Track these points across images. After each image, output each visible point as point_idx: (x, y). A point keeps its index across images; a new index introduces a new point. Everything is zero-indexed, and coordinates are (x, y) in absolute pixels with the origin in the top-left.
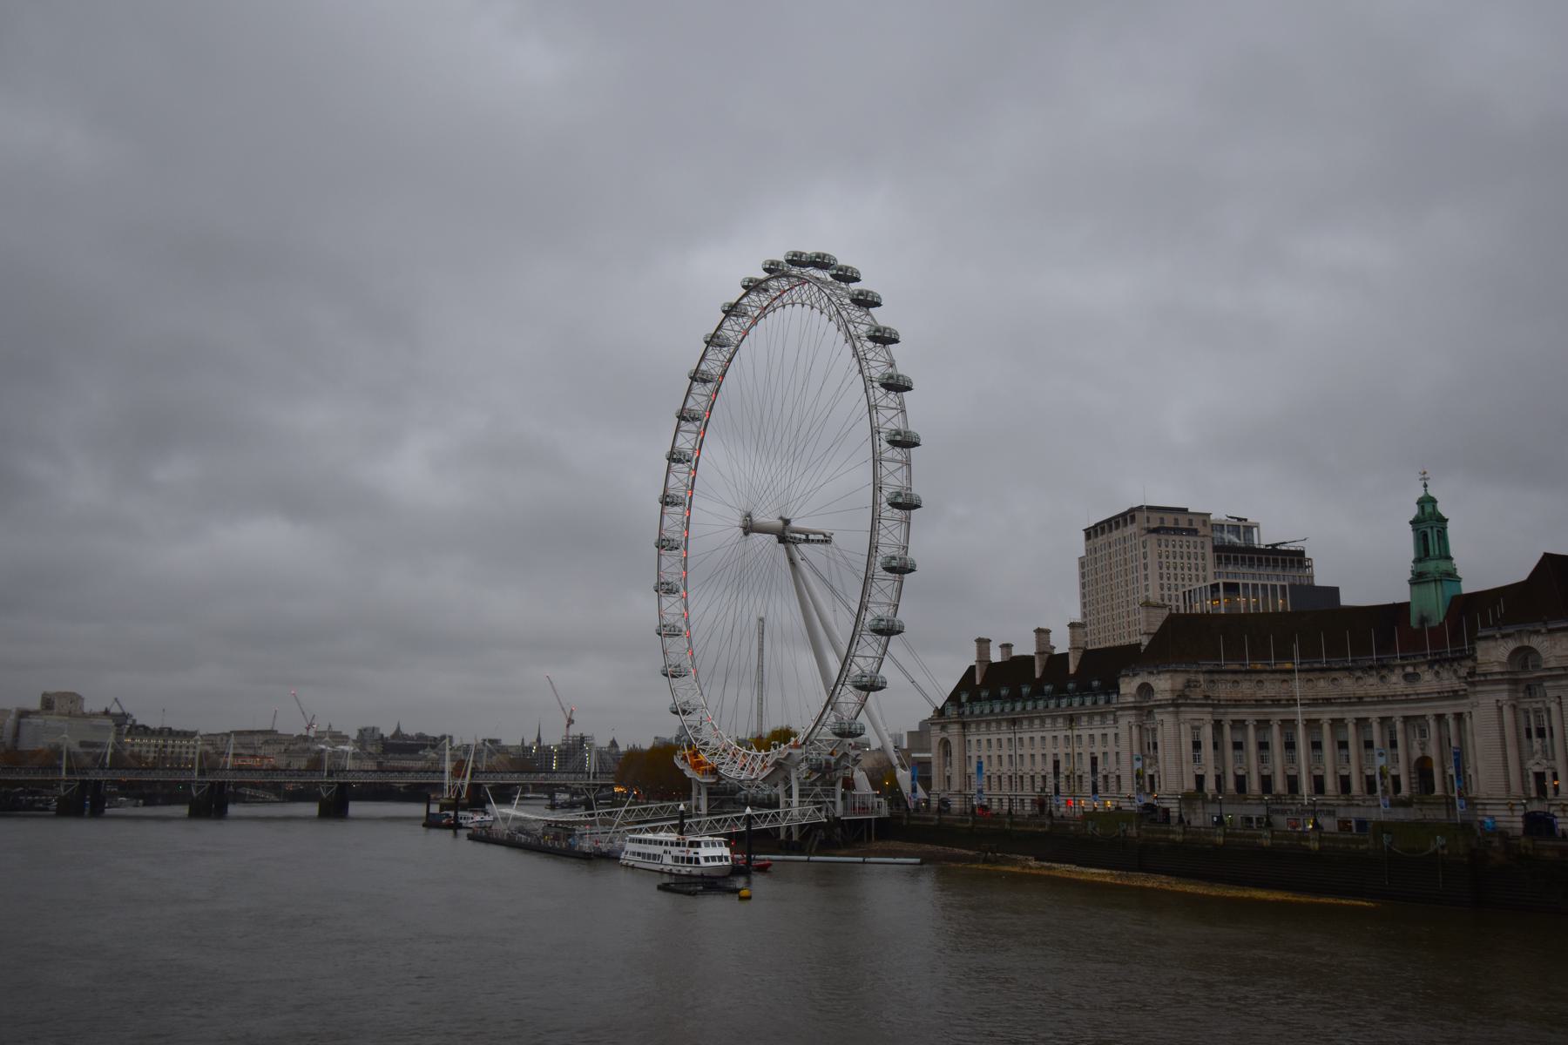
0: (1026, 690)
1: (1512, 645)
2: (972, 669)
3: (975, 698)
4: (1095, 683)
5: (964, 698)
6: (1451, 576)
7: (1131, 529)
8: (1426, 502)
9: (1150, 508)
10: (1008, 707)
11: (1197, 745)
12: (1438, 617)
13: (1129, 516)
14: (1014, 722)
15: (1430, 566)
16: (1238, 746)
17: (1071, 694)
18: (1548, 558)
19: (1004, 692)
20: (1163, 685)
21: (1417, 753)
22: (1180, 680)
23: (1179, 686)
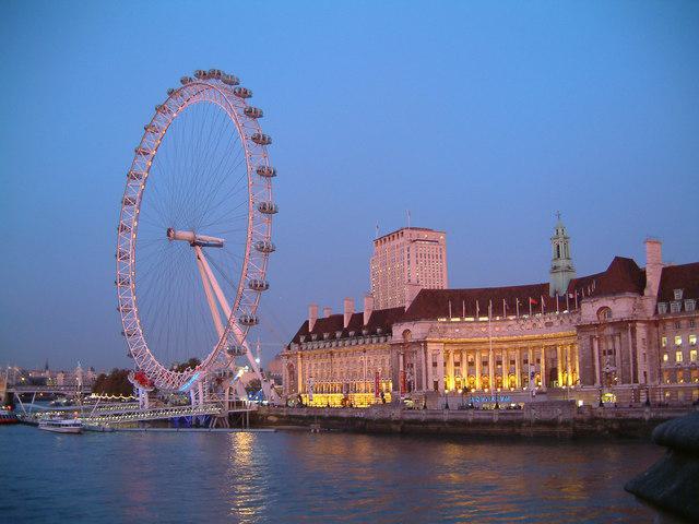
0: (338, 334)
1: (598, 305)
3: (308, 339)
7: (401, 240)
10: (328, 345)
11: (435, 365)
12: (563, 291)
13: (399, 233)
15: (562, 263)
16: (457, 364)
18: (617, 259)
20: (417, 330)
21: (550, 366)
23: (425, 330)
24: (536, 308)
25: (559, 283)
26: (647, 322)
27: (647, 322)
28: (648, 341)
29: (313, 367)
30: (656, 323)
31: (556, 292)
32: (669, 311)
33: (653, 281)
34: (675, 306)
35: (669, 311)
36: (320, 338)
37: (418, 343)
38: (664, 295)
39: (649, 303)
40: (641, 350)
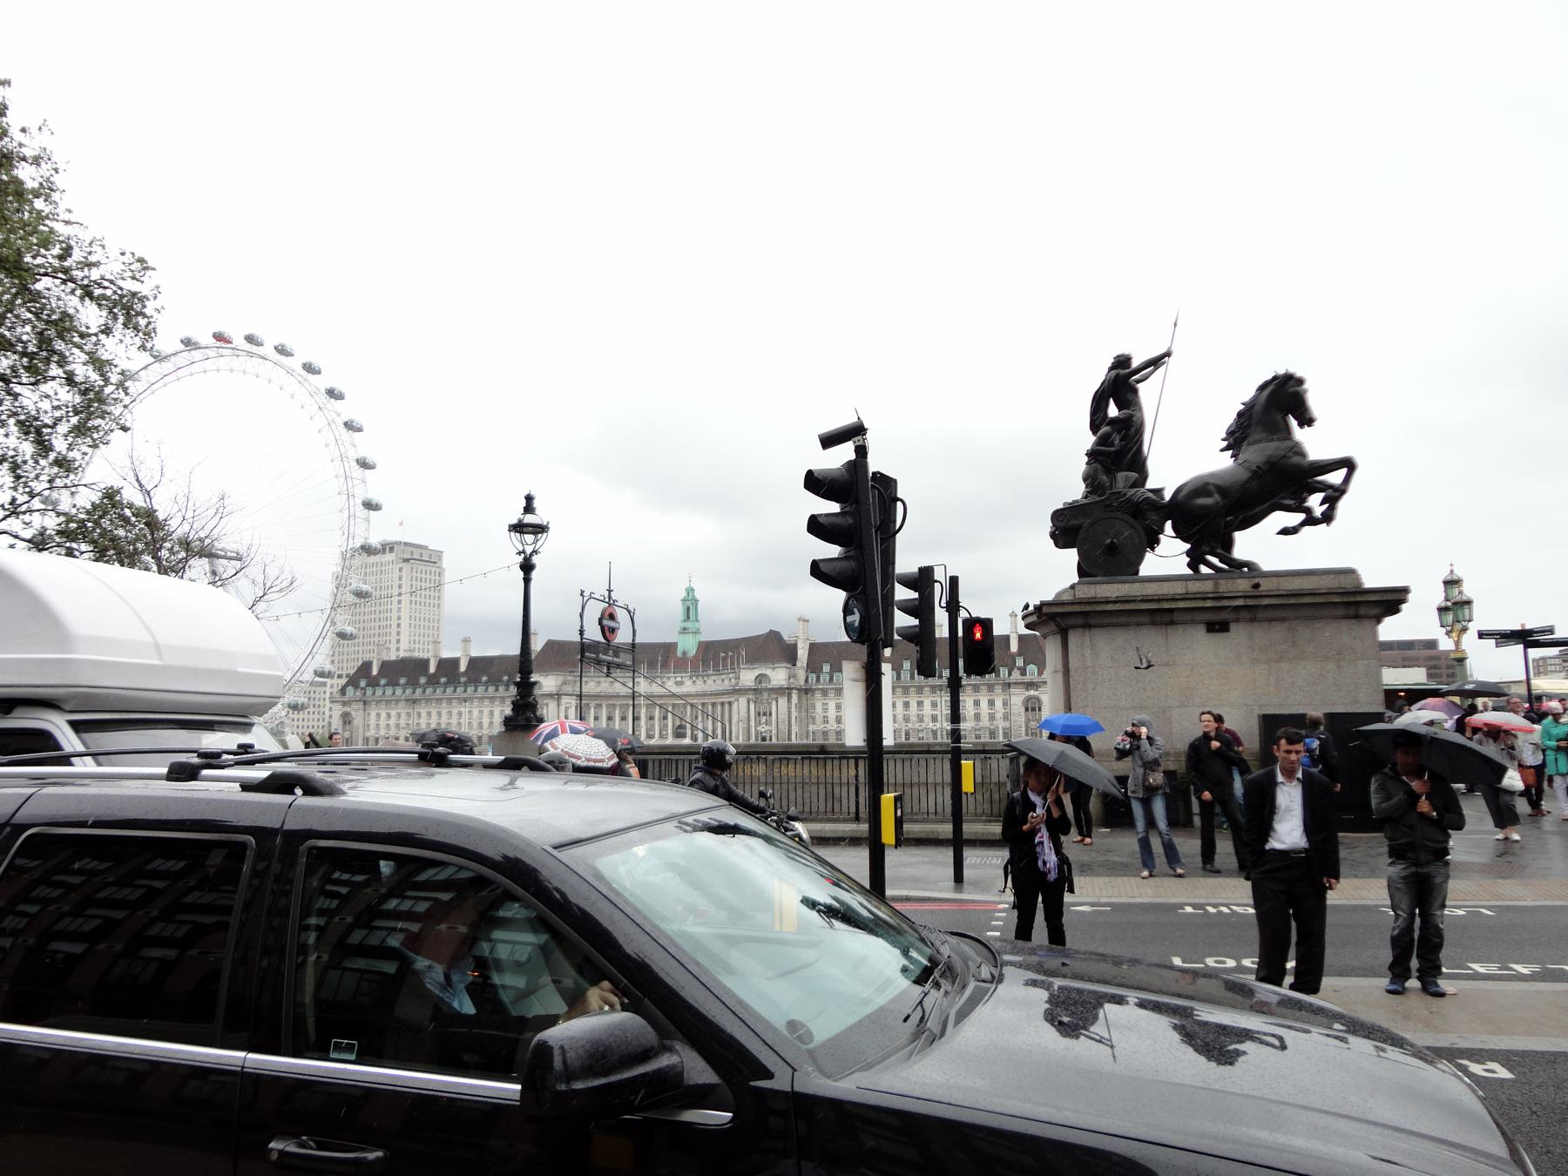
0: (423, 680)
1: (757, 672)
2: (366, 666)
3: (373, 683)
4: (484, 679)
5: (363, 683)
6: (697, 632)
7: (389, 557)
8: (690, 590)
9: (406, 544)
12: (692, 652)
14: (415, 701)
15: (689, 624)
17: (466, 685)
19: (403, 681)
21: (678, 723)
22: (561, 679)
24: (665, 666)
25: (688, 645)
26: (799, 690)
27: (799, 690)
28: (799, 706)
29: (383, 715)
30: (806, 691)
31: (684, 653)
32: (818, 680)
33: (803, 654)
34: (825, 677)
35: (818, 680)
36: (393, 683)
37: (551, 696)
38: (813, 667)
39: (801, 674)
40: (794, 714)
